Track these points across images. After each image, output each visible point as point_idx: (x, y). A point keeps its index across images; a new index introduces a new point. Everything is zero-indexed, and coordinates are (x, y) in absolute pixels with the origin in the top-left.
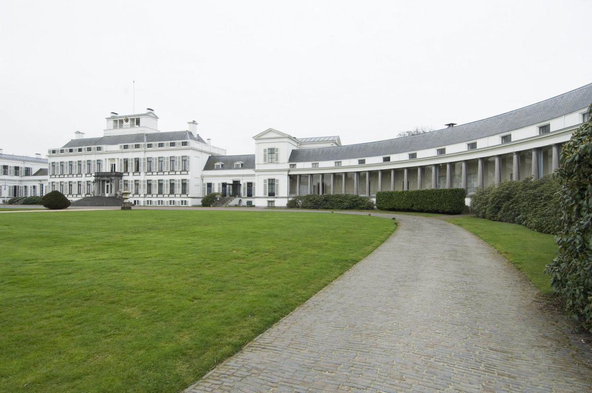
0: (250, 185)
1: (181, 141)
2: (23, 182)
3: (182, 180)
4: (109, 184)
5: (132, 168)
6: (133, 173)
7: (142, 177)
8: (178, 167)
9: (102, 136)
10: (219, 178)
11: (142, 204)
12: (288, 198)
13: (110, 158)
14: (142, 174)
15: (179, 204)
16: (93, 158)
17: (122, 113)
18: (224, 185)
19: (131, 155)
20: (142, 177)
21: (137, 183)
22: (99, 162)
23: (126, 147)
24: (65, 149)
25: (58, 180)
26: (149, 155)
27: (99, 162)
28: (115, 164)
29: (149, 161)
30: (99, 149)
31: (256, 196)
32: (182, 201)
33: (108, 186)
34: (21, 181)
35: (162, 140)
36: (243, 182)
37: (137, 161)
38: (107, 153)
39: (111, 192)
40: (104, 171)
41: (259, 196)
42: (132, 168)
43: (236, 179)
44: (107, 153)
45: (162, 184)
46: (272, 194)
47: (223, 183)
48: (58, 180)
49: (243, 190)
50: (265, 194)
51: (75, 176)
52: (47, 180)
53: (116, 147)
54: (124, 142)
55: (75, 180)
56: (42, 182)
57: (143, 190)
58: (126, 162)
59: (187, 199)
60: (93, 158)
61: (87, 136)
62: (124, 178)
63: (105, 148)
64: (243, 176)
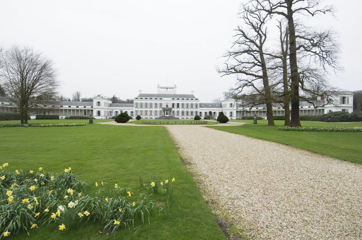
1: (182, 98)
4: (167, 112)
5: (176, 106)
7: (180, 110)
8: (149, 106)
10: (119, 110)
11: (181, 119)
13: (167, 102)
14: (180, 109)
16: (158, 102)
17: (160, 86)
18: (206, 113)
19: (176, 102)
20: (180, 110)
21: (178, 112)
22: (161, 104)
23: (173, 99)
25: (139, 110)
27: (161, 104)
28: (168, 105)
30: (161, 99)
33: (166, 113)
34: (108, 109)
36: (213, 112)
37: (178, 104)
38: (165, 100)
42: (176, 106)
43: (210, 111)
44: (165, 100)
45: (184, 112)
48: (139, 110)
49: (213, 114)
50: (97, 115)
51: (144, 108)
53: (170, 99)
54: (174, 97)
57: (180, 114)
58: (173, 105)
60: (158, 102)
61: (143, 93)
62: (173, 110)
63: (164, 99)
64: (124, 109)
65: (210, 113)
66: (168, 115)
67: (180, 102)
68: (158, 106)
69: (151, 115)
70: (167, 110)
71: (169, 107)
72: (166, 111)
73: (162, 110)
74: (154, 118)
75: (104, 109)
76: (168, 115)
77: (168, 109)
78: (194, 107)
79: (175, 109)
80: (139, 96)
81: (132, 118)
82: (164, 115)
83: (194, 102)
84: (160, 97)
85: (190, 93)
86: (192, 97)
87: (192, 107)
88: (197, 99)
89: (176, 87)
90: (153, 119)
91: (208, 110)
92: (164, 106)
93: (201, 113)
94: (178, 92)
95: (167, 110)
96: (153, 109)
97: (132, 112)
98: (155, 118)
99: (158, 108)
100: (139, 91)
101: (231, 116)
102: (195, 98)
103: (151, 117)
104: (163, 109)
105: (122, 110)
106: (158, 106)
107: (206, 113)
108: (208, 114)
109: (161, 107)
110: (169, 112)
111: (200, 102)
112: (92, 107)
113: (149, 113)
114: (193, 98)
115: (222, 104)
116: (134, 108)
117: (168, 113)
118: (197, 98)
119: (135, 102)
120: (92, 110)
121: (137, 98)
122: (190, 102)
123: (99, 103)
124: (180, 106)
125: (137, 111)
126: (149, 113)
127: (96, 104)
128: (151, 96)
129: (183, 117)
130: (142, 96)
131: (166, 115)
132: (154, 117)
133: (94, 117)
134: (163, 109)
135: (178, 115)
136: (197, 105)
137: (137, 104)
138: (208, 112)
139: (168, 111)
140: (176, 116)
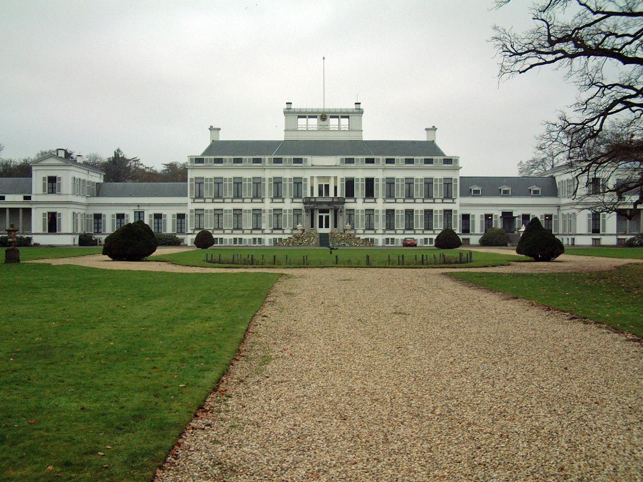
0: (466, 217)
2: (90, 208)
3: (253, 210)
4: (324, 215)
5: (360, 190)
6: (364, 199)
7: (380, 205)
9: (283, 140)
11: (380, 243)
12: (617, 235)
15: (231, 243)
16: (288, 174)
19: (360, 174)
20: (380, 205)
22: (298, 183)
23: (350, 161)
24: (205, 157)
25: (209, 206)
26: (390, 174)
27: (298, 183)
29: (390, 183)
31: (33, 232)
32: (426, 239)
33: (321, 217)
34: (88, 205)
35: (371, 154)
37: (370, 182)
38: (313, 167)
39: (336, 226)
40: (309, 195)
41: (37, 232)
42: (360, 190)
43: (507, 209)
44: (313, 167)
46: (596, 231)
47: (462, 215)
52: (186, 204)
55: (247, 206)
56: (141, 208)
57: (380, 225)
59: (396, 237)
60: (288, 174)
65: (508, 217)
66: (327, 226)
67: (379, 174)
68: (287, 191)
69: (257, 227)
70: (323, 207)
71: (332, 194)
72: (321, 211)
73: (300, 206)
74: (267, 239)
75: (72, 206)
76: (327, 226)
77: (329, 203)
78: (438, 192)
79: (359, 205)
80: (208, 151)
81: (183, 240)
82: (312, 226)
83: (438, 175)
84: (293, 150)
85: (422, 137)
86: (425, 151)
87: (428, 195)
88: (448, 161)
89: (360, 112)
90: (267, 243)
91: (496, 206)
92: (311, 190)
93: (466, 217)
94: (371, 132)
95: (325, 207)
96: (268, 205)
97: (181, 216)
98: (275, 240)
99: (288, 201)
100: (211, 129)
101: (596, 231)
102: (442, 158)
103: (257, 235)
104: (307, 201)
105: (141, 208)
106: (287, 191)
107: (488, 218)
108: (498, 224)
109: (297, 196)
110: (331, 215)
111: (463, 173)
112: (29, 198)
113: (248, 222)
114: (434, 158)
115: (558, 180)
116: (188, 200)
117: (327, 218)
118: (448, 153)
119: (191, 175)
120: (28, 212)
121: (199, 160)
122: (419, 175)
123: (52, 180)
124: (380, 190)
125: (199, 213)
126: (248, 222)
127: (44, 184)
128: (255, 151)
129: (390, 237)
130: (221, 151)
131: (321, 226)
132: (272, 237)
133: (36, 239)
134: (307, 201)
135: (370, 227)
136: (448, 183)
137: (200, 182)
138: (497, 213)
139: (327, 211)
140: (361, 233)
